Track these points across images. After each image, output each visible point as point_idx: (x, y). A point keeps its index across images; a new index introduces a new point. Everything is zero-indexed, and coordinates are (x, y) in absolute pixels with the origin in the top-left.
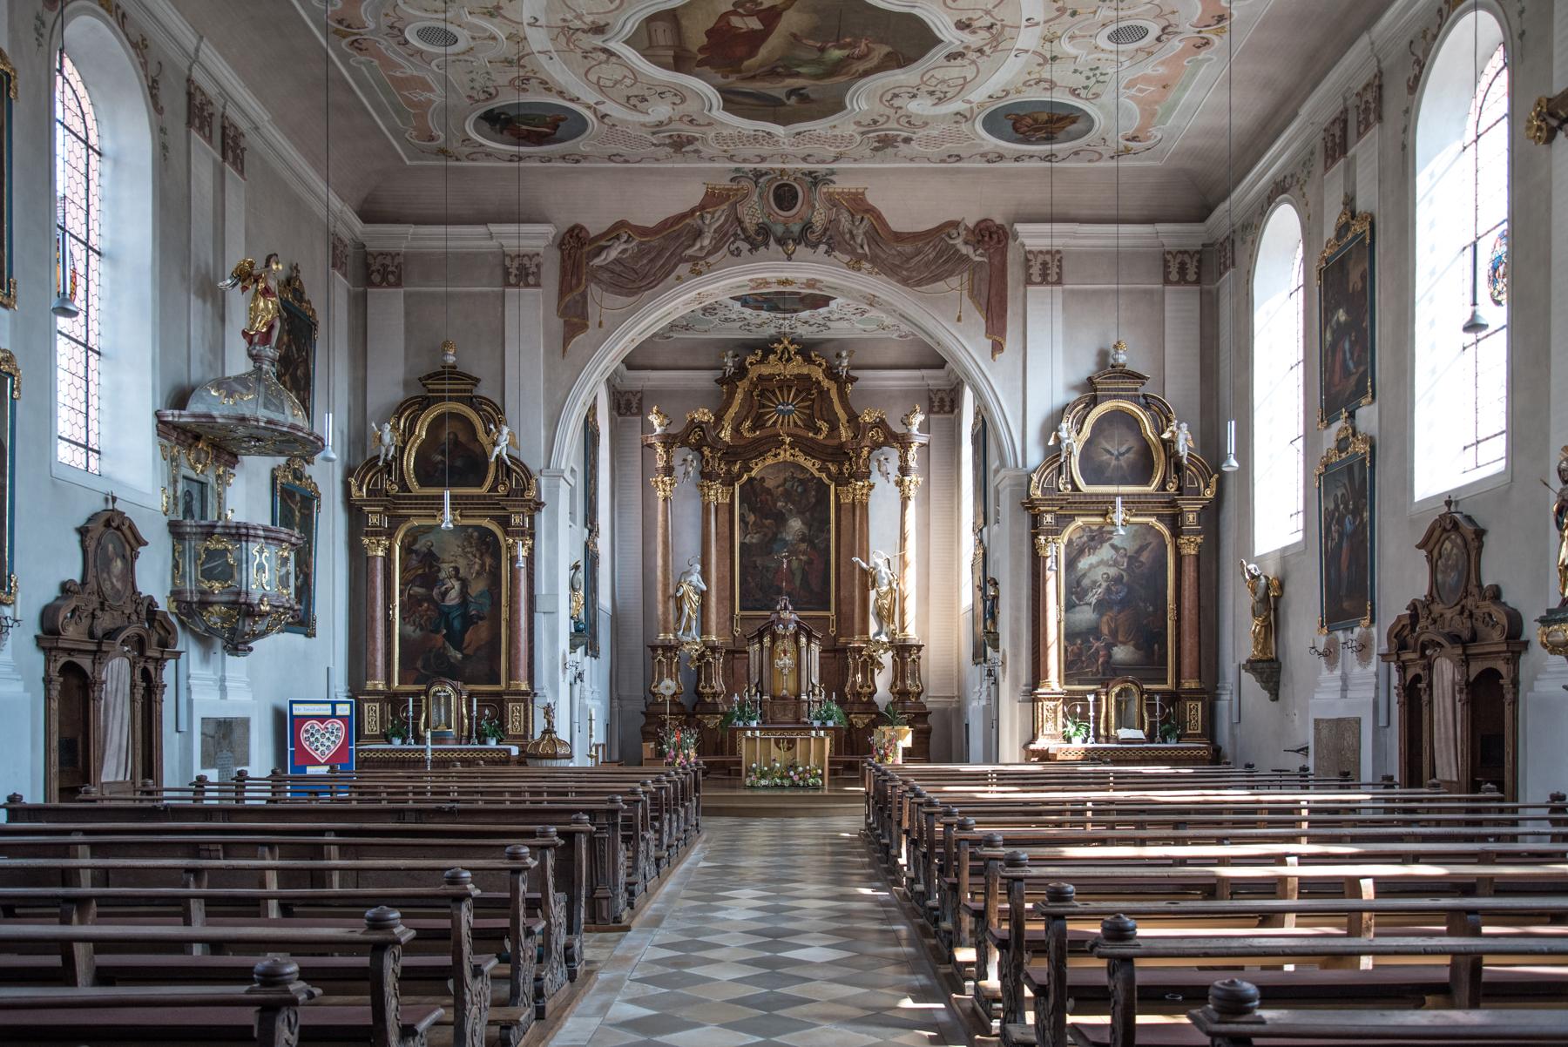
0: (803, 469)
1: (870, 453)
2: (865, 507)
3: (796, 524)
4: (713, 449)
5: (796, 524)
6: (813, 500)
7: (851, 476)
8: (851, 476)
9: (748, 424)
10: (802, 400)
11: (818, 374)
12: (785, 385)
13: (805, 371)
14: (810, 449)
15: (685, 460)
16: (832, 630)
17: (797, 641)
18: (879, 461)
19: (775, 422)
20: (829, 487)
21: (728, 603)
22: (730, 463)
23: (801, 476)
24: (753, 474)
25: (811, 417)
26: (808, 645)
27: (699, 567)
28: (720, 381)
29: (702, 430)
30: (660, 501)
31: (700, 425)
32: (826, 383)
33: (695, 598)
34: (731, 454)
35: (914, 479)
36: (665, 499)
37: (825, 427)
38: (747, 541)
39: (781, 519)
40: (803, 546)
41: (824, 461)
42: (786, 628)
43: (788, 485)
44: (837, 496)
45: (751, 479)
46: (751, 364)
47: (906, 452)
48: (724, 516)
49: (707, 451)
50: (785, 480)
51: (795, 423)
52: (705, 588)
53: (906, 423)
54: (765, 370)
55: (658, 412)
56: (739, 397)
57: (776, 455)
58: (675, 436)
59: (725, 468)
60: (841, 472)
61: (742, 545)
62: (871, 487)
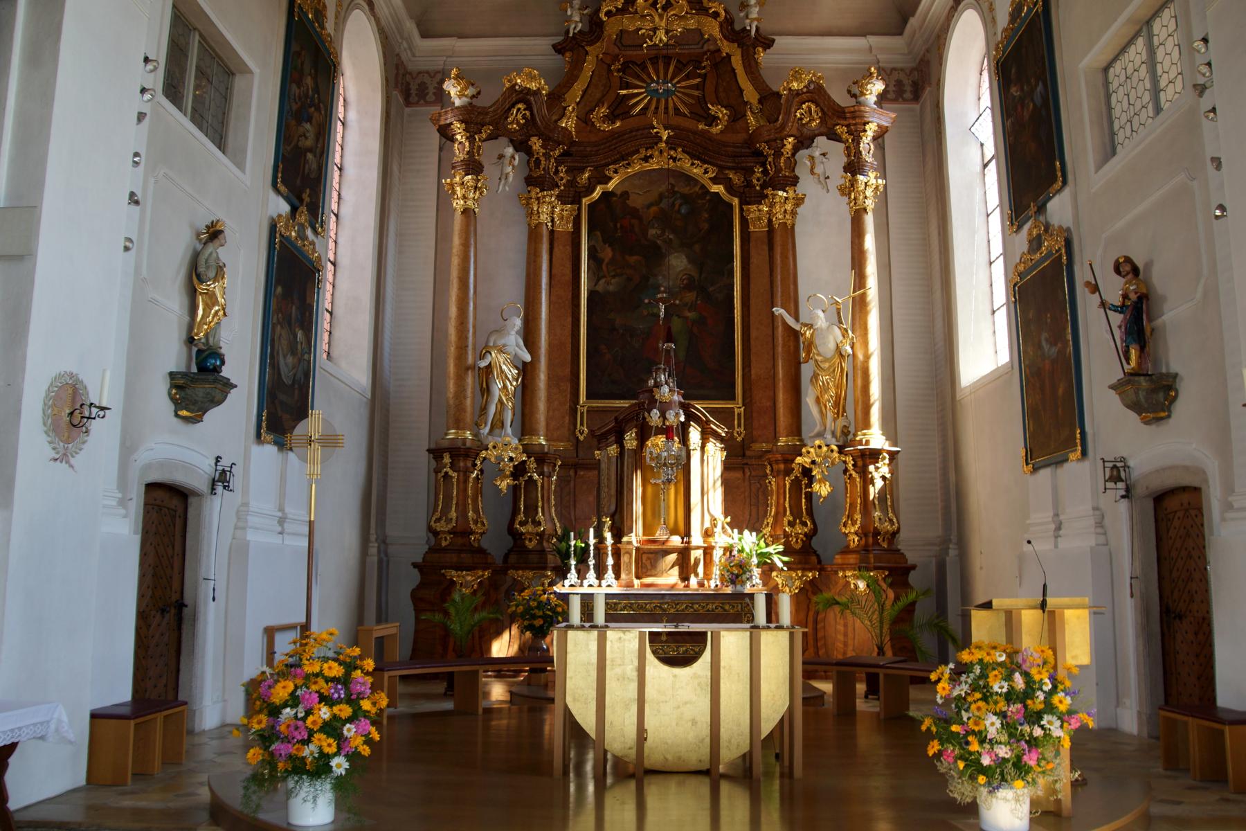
0: (690, 180)
1: (796, 149)
2: (789, 231)
3: (678, 263)
4: (547, 141)
5: (678, 263)
6: (706, 226)
7: (764, 187)
8: (764, 187)
9: (603, 111)
10: (687, 77)
11: (713, 29)
12: (660, 57)
13: (692, 23)
14: (701, 149)
15: (501, 157)
16: (739, 432)
17: (685, 441)
18: (812, 158)
19: (645, 109)
20: (730, 206)
21: (567, 387)
22: (575, 171)
23: (686, 190)
24: (611, 186)
25: (702, 102)
26: (703, 447)
27: (518, 323)
28: (559, 49)
29: (529, 107)
30: (458, 215)
31: (524, 96)
32: (726, 47)
33: (511, 372)
34: (575, 155)
35: (870, 180)
36: (466, 211)
37: (722, 113)
38: (600, 287)
39: (654, 255)
40: (690, 296)
41: (721, 168)
42: (663, 416)
43: (663, 205)
44: (744, 222)
45: (605, 195)
46: (609, 14)
47: (857, 140)
48: (563, 251)
49: (536, 144)
50: (661, 197)
51: (676, 109)
52: (528, 358)
53: (856, 95)
54: (628, 23)
55: (458, 77)
56: (589, 67)
57: (646, 159)
58: (483, 111)
59: (566, 178)
60: (749, 185)
61: (592, 295)
62: (799, 201)
